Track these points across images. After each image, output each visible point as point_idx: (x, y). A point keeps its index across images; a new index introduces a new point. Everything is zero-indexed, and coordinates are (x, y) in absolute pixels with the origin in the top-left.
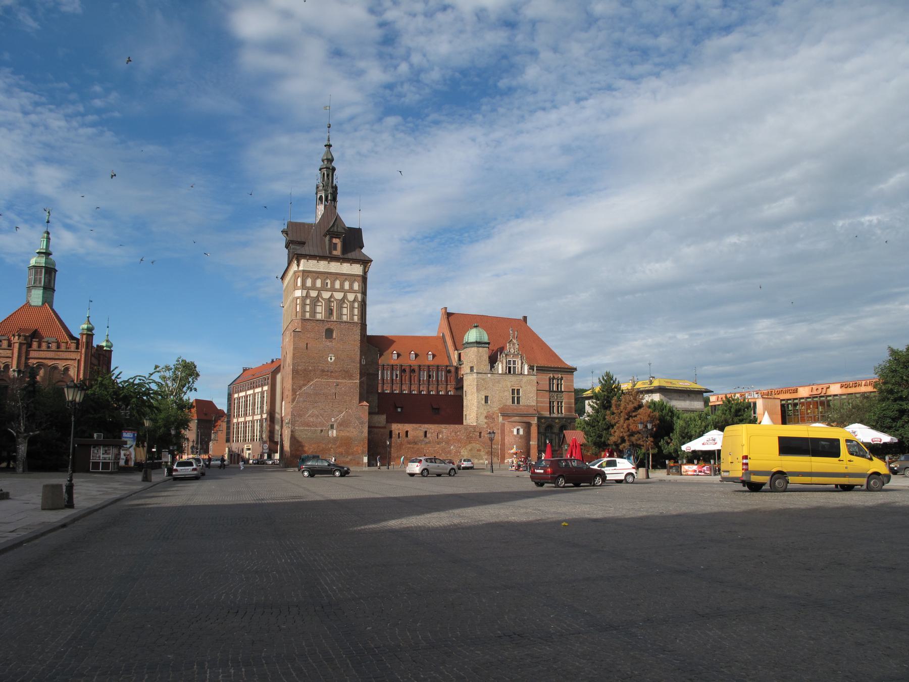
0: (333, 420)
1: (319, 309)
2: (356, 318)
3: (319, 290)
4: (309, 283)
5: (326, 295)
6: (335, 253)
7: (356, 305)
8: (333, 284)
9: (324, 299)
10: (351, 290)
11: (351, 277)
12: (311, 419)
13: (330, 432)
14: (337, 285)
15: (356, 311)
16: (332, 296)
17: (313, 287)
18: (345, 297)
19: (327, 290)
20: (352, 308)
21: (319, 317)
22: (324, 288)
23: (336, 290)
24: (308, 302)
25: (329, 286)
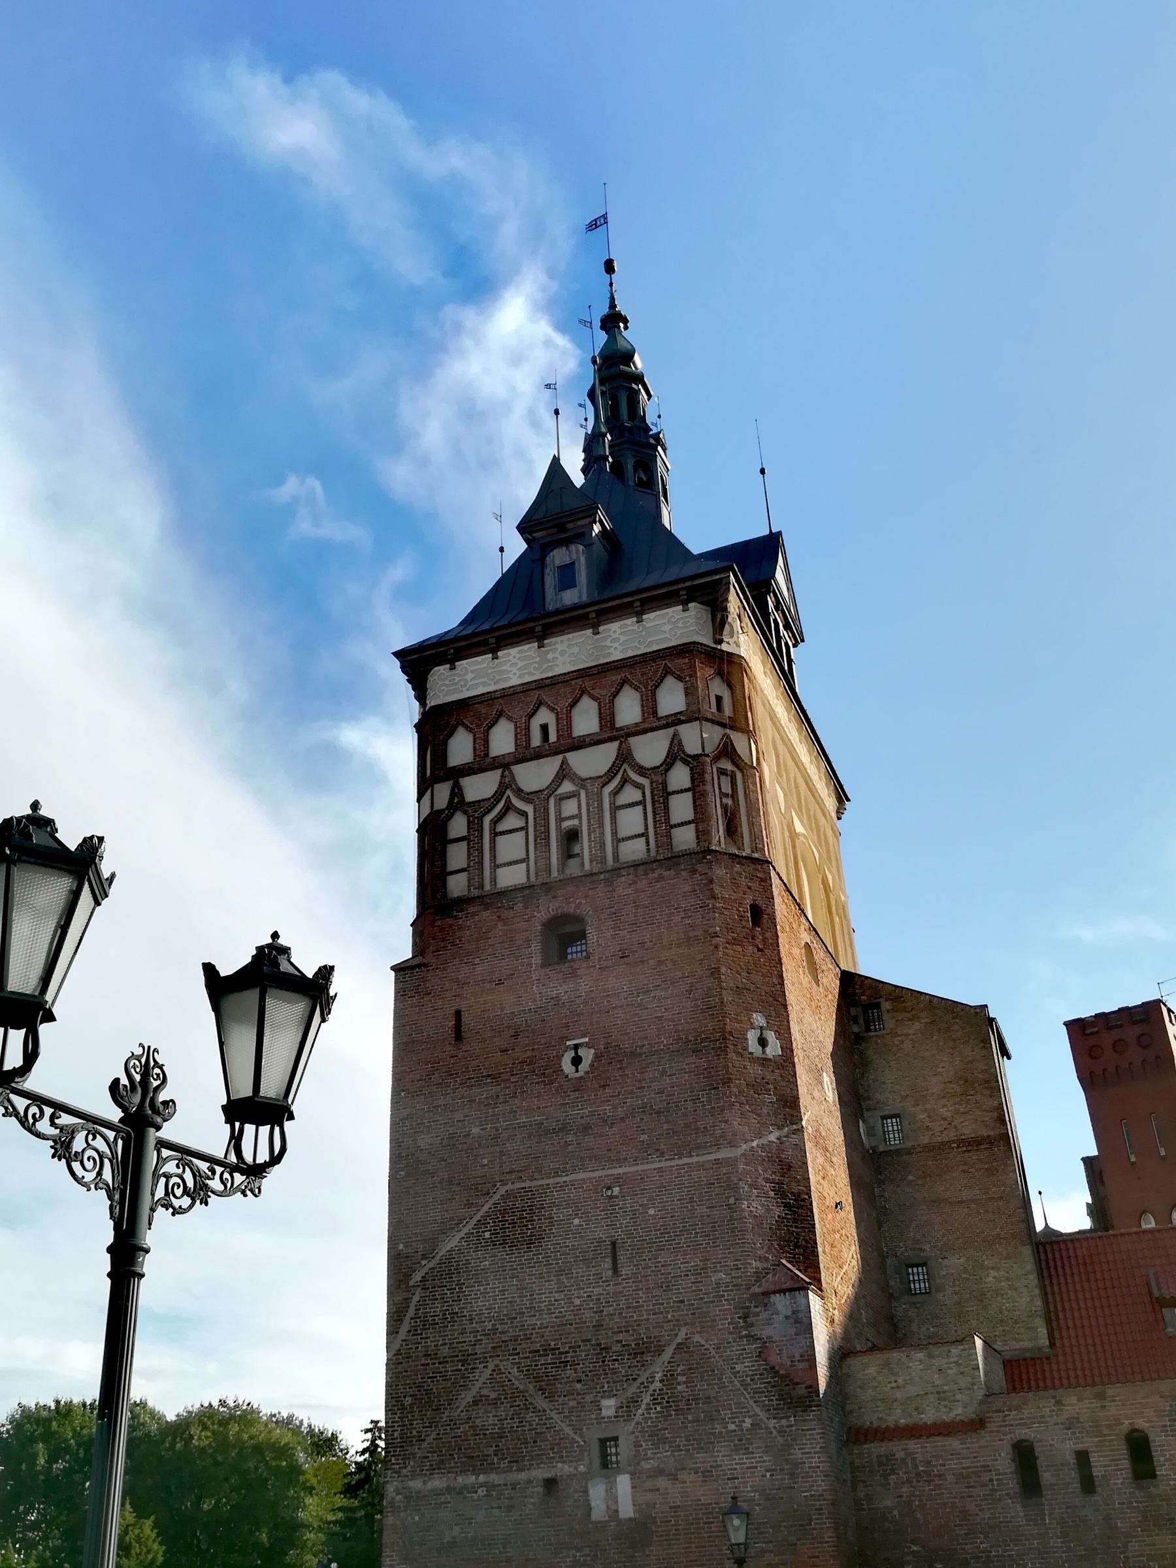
0: (609, 1406)
1: (511, 847)
2: (685, 838)
3: (504, 764)
4: (461, 748)
5: (534, 776)
6: (570, 597)
7: (680, 776)
8: (565, 723)
9: (527, 797)
10: (652, 721)
11: (646, 670)
12: (488, 1419)
13: (597, 1493)
14: (586, 720)
15: (681, 807)
16: (564, 773)
17: (482, 763)
18: (625, 757)
19: (538, 755)
20: (662, 795)
21: (512, 877)
22: (525, 754)
23: (581, 744)
24: (458, 826)
25: (553, 737)
